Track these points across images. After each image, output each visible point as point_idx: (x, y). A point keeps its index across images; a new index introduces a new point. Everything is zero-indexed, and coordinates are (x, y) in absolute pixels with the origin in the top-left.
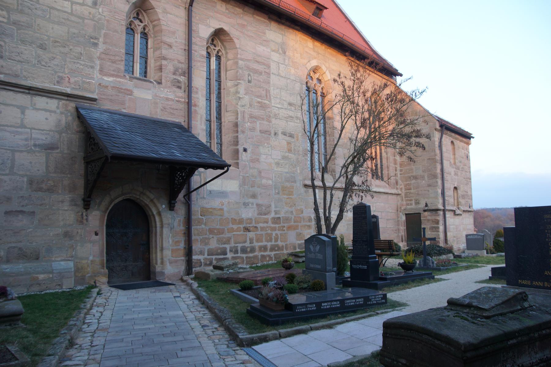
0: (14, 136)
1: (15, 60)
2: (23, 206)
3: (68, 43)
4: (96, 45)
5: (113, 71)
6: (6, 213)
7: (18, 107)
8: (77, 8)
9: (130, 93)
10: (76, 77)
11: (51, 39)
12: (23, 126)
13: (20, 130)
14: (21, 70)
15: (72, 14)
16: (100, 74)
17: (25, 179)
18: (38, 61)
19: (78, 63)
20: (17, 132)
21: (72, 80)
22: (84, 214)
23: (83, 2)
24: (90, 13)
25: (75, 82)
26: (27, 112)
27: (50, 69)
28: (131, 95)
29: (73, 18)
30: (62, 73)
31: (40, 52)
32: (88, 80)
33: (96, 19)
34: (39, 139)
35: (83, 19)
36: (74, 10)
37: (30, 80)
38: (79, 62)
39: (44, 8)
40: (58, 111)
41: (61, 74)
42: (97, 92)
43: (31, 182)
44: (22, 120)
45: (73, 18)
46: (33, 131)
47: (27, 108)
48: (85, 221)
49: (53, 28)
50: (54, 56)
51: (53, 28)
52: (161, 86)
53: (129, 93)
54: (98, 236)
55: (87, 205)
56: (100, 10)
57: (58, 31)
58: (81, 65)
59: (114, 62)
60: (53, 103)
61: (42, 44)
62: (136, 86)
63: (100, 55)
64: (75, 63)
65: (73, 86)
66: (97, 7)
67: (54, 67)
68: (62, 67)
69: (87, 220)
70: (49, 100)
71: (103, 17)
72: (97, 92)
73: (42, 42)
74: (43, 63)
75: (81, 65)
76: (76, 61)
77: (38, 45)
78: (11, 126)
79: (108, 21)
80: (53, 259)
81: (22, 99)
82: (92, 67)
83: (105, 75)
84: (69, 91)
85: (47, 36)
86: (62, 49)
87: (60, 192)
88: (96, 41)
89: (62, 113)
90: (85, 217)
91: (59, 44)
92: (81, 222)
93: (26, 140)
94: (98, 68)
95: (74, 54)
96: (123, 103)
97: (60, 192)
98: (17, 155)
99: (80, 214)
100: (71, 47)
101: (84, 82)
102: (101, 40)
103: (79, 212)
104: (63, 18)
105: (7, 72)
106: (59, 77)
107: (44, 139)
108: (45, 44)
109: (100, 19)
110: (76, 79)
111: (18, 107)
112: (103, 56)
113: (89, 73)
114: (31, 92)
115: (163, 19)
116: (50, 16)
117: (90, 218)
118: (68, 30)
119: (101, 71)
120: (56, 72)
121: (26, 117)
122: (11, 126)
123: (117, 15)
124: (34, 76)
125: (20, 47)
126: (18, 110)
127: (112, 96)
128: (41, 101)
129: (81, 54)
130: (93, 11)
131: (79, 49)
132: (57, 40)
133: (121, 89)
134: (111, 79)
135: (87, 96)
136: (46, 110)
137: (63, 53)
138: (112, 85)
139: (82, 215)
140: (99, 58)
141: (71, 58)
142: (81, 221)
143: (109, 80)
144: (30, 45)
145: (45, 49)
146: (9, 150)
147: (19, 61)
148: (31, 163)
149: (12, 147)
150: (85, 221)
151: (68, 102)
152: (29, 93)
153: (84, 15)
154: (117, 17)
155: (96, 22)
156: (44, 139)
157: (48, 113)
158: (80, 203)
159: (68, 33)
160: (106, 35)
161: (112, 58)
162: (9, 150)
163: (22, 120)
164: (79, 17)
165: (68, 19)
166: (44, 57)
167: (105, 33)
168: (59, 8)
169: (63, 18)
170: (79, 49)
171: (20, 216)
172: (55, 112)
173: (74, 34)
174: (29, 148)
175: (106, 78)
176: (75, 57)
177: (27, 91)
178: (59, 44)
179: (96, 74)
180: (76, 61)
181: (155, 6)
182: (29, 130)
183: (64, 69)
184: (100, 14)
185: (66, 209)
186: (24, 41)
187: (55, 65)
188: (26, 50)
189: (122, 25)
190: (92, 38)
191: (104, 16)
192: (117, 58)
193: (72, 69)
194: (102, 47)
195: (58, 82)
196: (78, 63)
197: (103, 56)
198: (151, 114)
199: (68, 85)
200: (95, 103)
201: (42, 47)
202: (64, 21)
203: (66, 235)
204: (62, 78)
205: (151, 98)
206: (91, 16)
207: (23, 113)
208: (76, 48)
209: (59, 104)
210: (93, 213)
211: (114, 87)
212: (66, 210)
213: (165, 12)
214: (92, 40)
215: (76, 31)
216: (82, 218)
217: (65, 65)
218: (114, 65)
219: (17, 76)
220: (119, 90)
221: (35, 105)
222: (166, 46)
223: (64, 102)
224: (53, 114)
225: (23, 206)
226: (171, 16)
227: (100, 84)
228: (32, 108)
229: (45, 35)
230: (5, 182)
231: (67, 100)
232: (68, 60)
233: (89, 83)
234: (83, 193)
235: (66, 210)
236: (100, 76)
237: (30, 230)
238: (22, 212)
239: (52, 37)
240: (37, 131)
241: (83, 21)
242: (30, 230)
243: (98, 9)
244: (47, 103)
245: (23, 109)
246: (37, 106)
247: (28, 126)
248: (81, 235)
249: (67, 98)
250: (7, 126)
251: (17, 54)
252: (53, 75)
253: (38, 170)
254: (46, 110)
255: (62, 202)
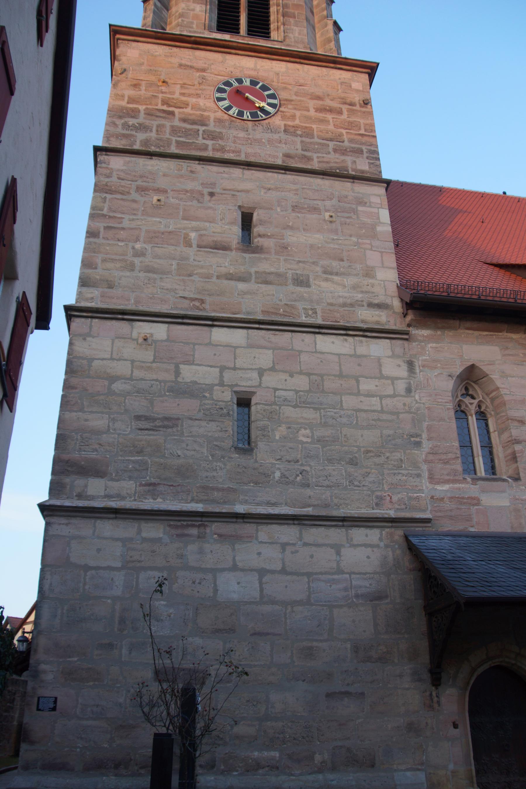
0: (331, 586)
1: (323, 486)
2: (348, 684)
3: (383, 450)
4: (418, 444)
5: (448, 475)
6: (329, 695)
7: (332, 546)
8: (387, 402)
9: (476, 501)
10: (399, 493)
11: (362, 449)
12: (340, 571)
13: (336, 577)
14: (331, 497)
15: (382, 411)
16: (430, 483)
17: (349, 646)
18: (350, 482)
19: (399, 473)
20: (334, 579)
21: (395, 498)
22: (434, 694)
23: (394, 393)
24: (404, 405)
25: (399, 500)
26: (343, 551)
27: (365, 488)
28: (478, 504)
29: (384, 417)
30: (381, 490)
31: (351, 469)
32: (415, 495)
33: (413, 410)
34: (361, 587)
35: (397, 414)
36: (384, 405)
37: (343, 508)
38: (401, 471)
39: (350, 412)
40: (382, 544)
41: (379, 493)
42: (429, 509)
43: (356, 649)
44: (338, 563)
45: (384, 417)
46: (353, 576)
47: (343, 546)
48: (436, 705)
49: (362, 436)
50: (368, 470)
51: (362, 436)
52: (520, 483)
53: (476, 502)
54: (457, 730)
55: (436, 681)
56: (417, 397)
57: (369, 437)
58: (403, 475)
59: (446, 462)
60: (373, 535)
61: (351, 459)
62: (483, 491)
63: (426, 456)
64: (395, 474)
65: (397, 506)
66: (413, 394)
67: (370, 485)
68: (380, 483)
69: (438, 703)
70: (368, 531)
71: (422, 405)
72: (429, 509)
73: (351, 457)
74: (356, 483)
75: (403, 475)
76: (396, 471)
77: (347, 460)
78: (325, 573)
79: (429, 409)
80: (395, 767)
81: (335, 535)
82: (419, 476)
83: (438, 483)
84: (392, 514)
85: (357, 447)
86: (377, 460)
87: (396, 661)
88: (418, 439)
89: (387, 546)
90: (435, 699)
91: (372, 454)
92: (431, 707)
93: (346, 589)
94: (426, 474)
95: (392, 462)
96: (469, 519)
97: (396, 661)
98: (336, 611)
99: (428, 693)
100: (388, 454)
101: (410, 498)
102: (424, 436)
103: (426, 691)
104: (373, 420)
105: (316, 503)
106: (377, 497)
107: (368, 585)
108: (356, 457)
109: (418, 409)
110: (399, 496)
111: (332, 546)
112: (431, 457)
113: (415, 484)
114: (345, 523)
115: (503, 386)
116: (357, 421)
117: (443, 700)
118: (381, 433)
119: (432, 479)
120: (373, 492)
121: (342, 558)
122: (325, 573)
123: (440, 397)
124: (347, 502)
125: (327, 468)
126: (333, 550)
127: (451, 510)
128: (359, 534)
129: (401, 460)
130: (408, 400)
131: (398, 455)
132: (369, 449)
133: (463, 498)
134: (446, 487)
135: (418, 516)
136: (366, 545)
137: (378, 465)
138: (449, 495)
139: (431, 695)
140: (426, 461)
141: (389, 470)
142: (431, 705)
143: (444, 488)
144: (338, 463)
145: (356, 464)
146: (325, 606)
147: (328, 486)
148: (354, 621)
149: (329, 601)
150: (436, 705)
151: (393, 530)
152: (343, 526)
153: (397, 409)
154: (440, 400)
155: (414, 413)
156: (368, 585)
157: (369, 549)
158: (426, 676)
159: (381, 436)
160: (429, 429)
161: (444, 457)
162: (325, 606)
163: (338, 563)
164: (392, 413)
165: (379, 420)
166: (356, 474)
167: (428, 425)
168: (366, 408)
169: (373, 420)
170: (398, 455)
171: (346, 699)
172: (378, 546)
173: (389, 436)
174: (349, 601)
175: (439, 487)
176: (394, 466)
177: (341, 523)
178: (372, 454)
179: (425, 484)
180: (396, 471)
181: (488, 372)
182: (348, 576)
183: (383, 485)
184: (417, 402)
185: (407, 686)
186: (330, 460)
187: (370, 482)
188: (334, 470)
189: (448, 409)
190: (412, 436)
191: (424, 404)
192: (450, 456)
193: (392, 484)
194: (426, 445)
195: (377, 504)
196: (399, 473)
197: (431, 457)
198: (512, 528)
199: (390, 507)
200: (429, 525)
201: (353, 462)
202: (374, 423)
203: (412, 728)
204: (381, 498)
205: (508, 504)
206: (407, 408)
207: (338, 553)
208: (394, 454)
209: (381, 534)
210: (447, 692)
211: (452, 498)
212: (408, 689)
213: (504, 375)
214: (412, 439)
215: (391, 432)
216: (432, 700)
217: (383, 479)
218: (447, 466)
219: (327, 506)
220: (460, 500)
221: (352, 539)
222: (516, 424)
223: (387, 530)
224: (375, 549)
225: (348, 684)
226: (514, 379)
227: (432, 497)
228: (348, 545)
229: (354, 446)
230: (324, 650)
231: (392, 527)
232: (386, 472)
233: (417, 498)
234: (428, 661)
235: (408, 689)
236: (430, 486)
237: (360, 721)
238: (347, 694)
239: (363, 447)
240: (358, 576)
241: (398, 417)
242: (360, 721)
243: (414, 397)
244: (367, 536)
245: (337, 548)
246: (355, 542)
247: (346, 571)
248: (433, 729)
249: (390, 525)
250: (321, 573)
251: (325, 478)
252: (369, 496)
253: (365, 631)
254: (366, 545)
255: (401, 676)
